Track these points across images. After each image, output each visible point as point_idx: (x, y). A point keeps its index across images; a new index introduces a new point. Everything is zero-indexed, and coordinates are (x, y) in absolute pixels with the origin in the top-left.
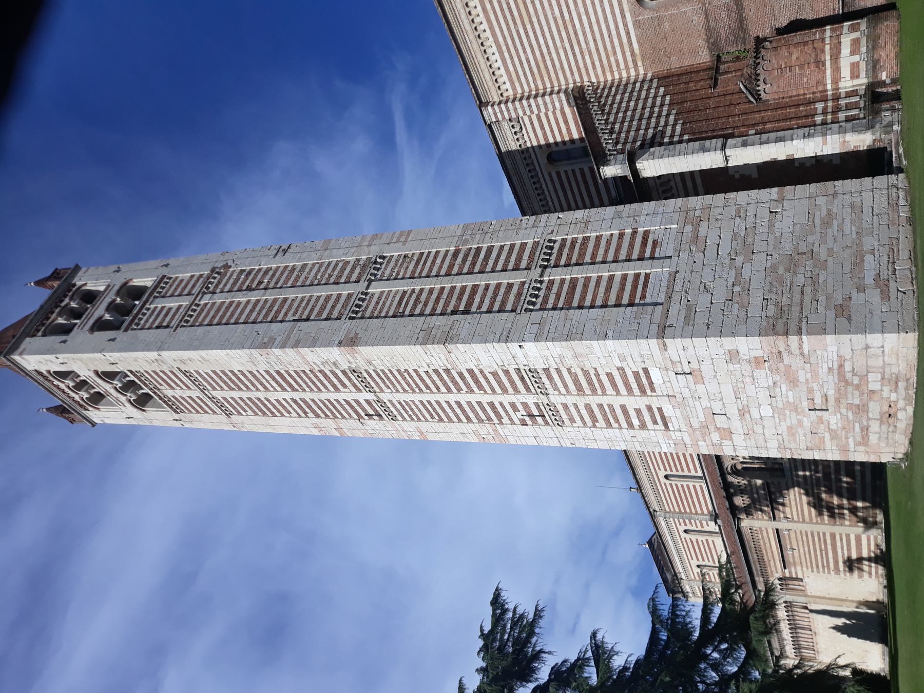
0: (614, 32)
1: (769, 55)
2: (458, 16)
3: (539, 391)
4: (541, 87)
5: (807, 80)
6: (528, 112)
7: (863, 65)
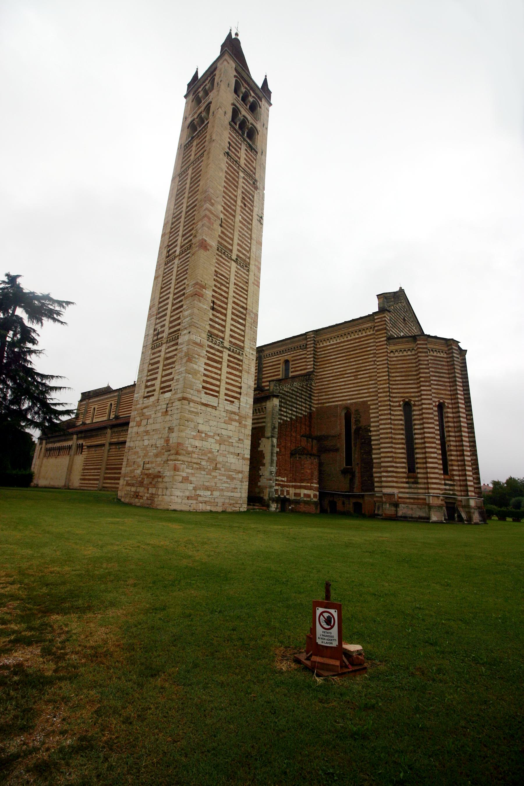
0: (335, 396)
3: (169, 339)
7: (298, 498)
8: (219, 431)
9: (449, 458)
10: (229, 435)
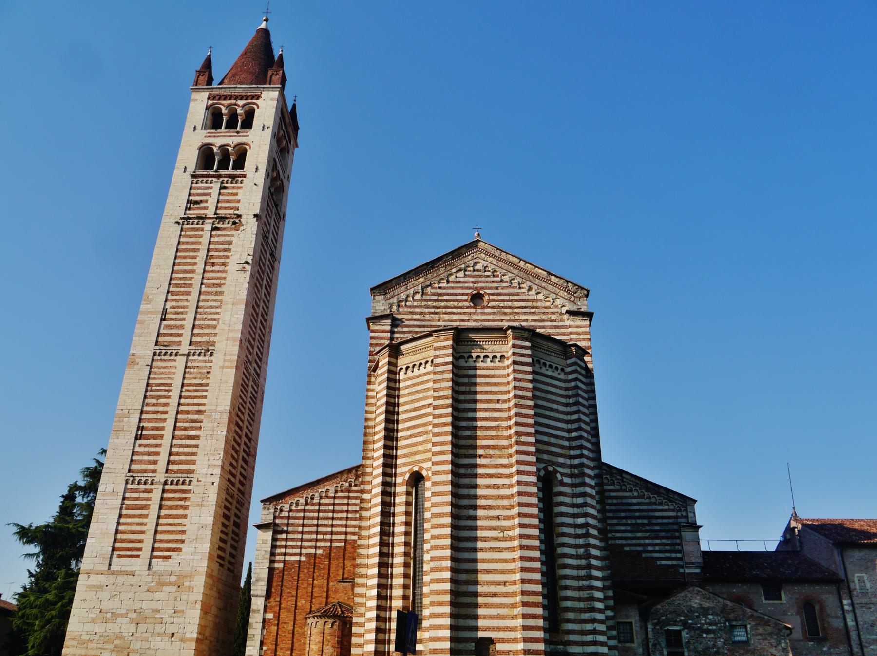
8: (137, 606)
10: (156, 607)
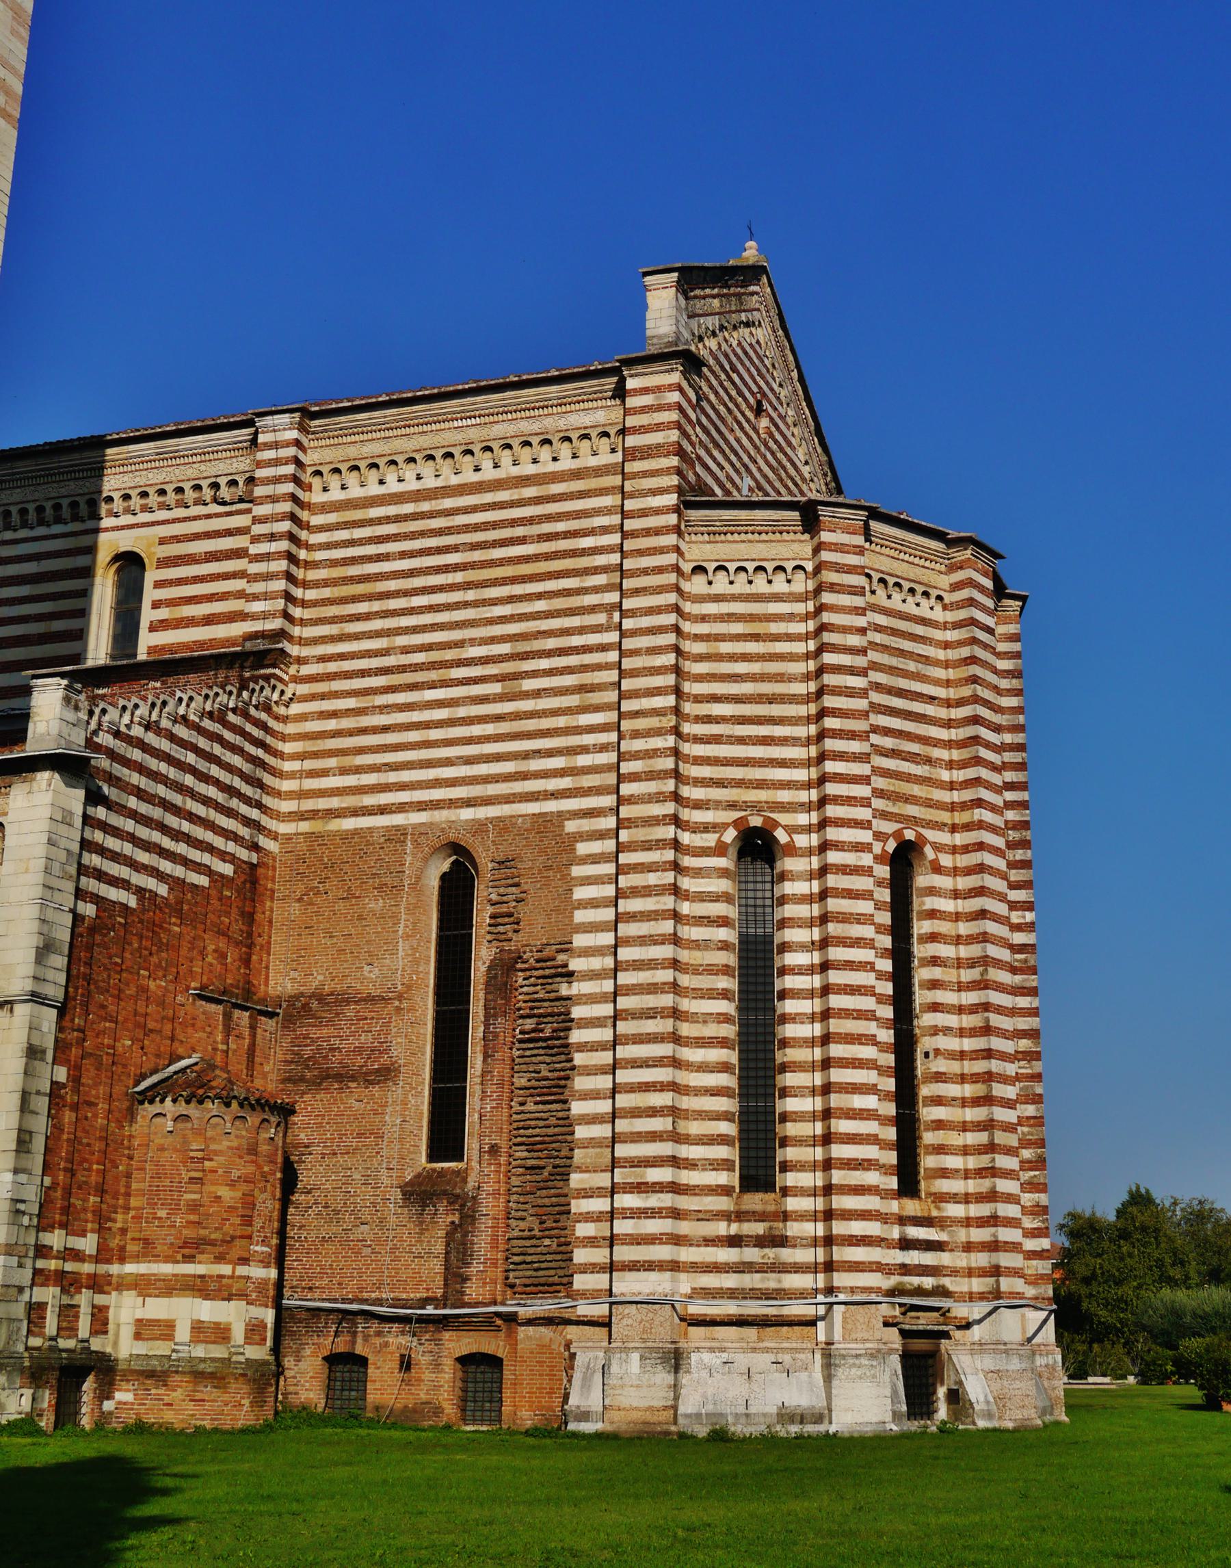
0: (393, 777)
1: (244, 1133)
2: (528, 413)
4: (312, 575)
5: (160, 1218)
6: (258, 529)
7: (161, 1348)
9: (928, 1113)
